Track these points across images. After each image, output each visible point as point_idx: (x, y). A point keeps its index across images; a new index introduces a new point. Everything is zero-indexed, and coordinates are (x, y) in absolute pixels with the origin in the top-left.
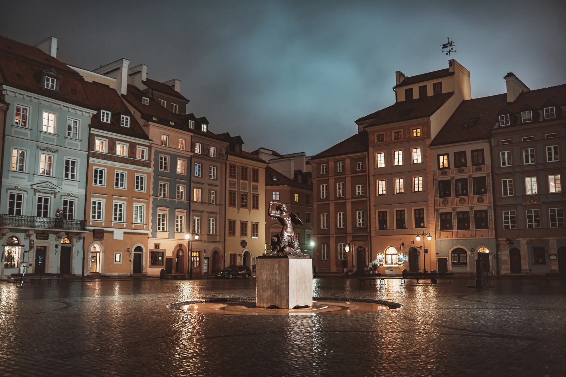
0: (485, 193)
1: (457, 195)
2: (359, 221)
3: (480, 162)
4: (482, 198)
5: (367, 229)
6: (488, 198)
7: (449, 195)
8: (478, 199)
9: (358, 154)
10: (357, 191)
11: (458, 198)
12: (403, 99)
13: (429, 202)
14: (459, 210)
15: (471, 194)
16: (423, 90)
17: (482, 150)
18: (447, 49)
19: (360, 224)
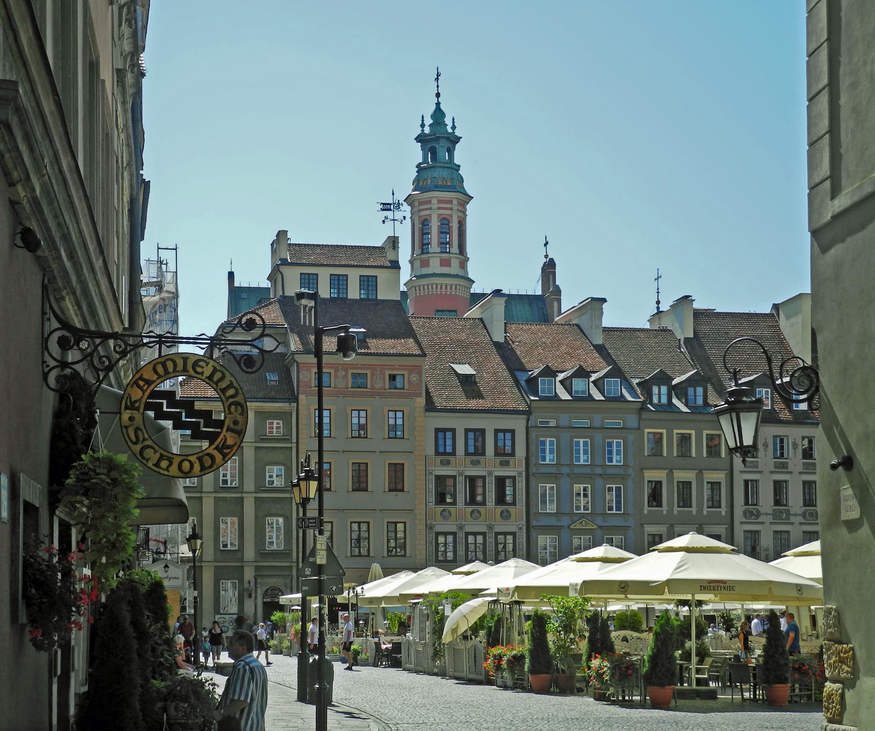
0: (514, 503)
4: (508, 511)
8: (502, 512)
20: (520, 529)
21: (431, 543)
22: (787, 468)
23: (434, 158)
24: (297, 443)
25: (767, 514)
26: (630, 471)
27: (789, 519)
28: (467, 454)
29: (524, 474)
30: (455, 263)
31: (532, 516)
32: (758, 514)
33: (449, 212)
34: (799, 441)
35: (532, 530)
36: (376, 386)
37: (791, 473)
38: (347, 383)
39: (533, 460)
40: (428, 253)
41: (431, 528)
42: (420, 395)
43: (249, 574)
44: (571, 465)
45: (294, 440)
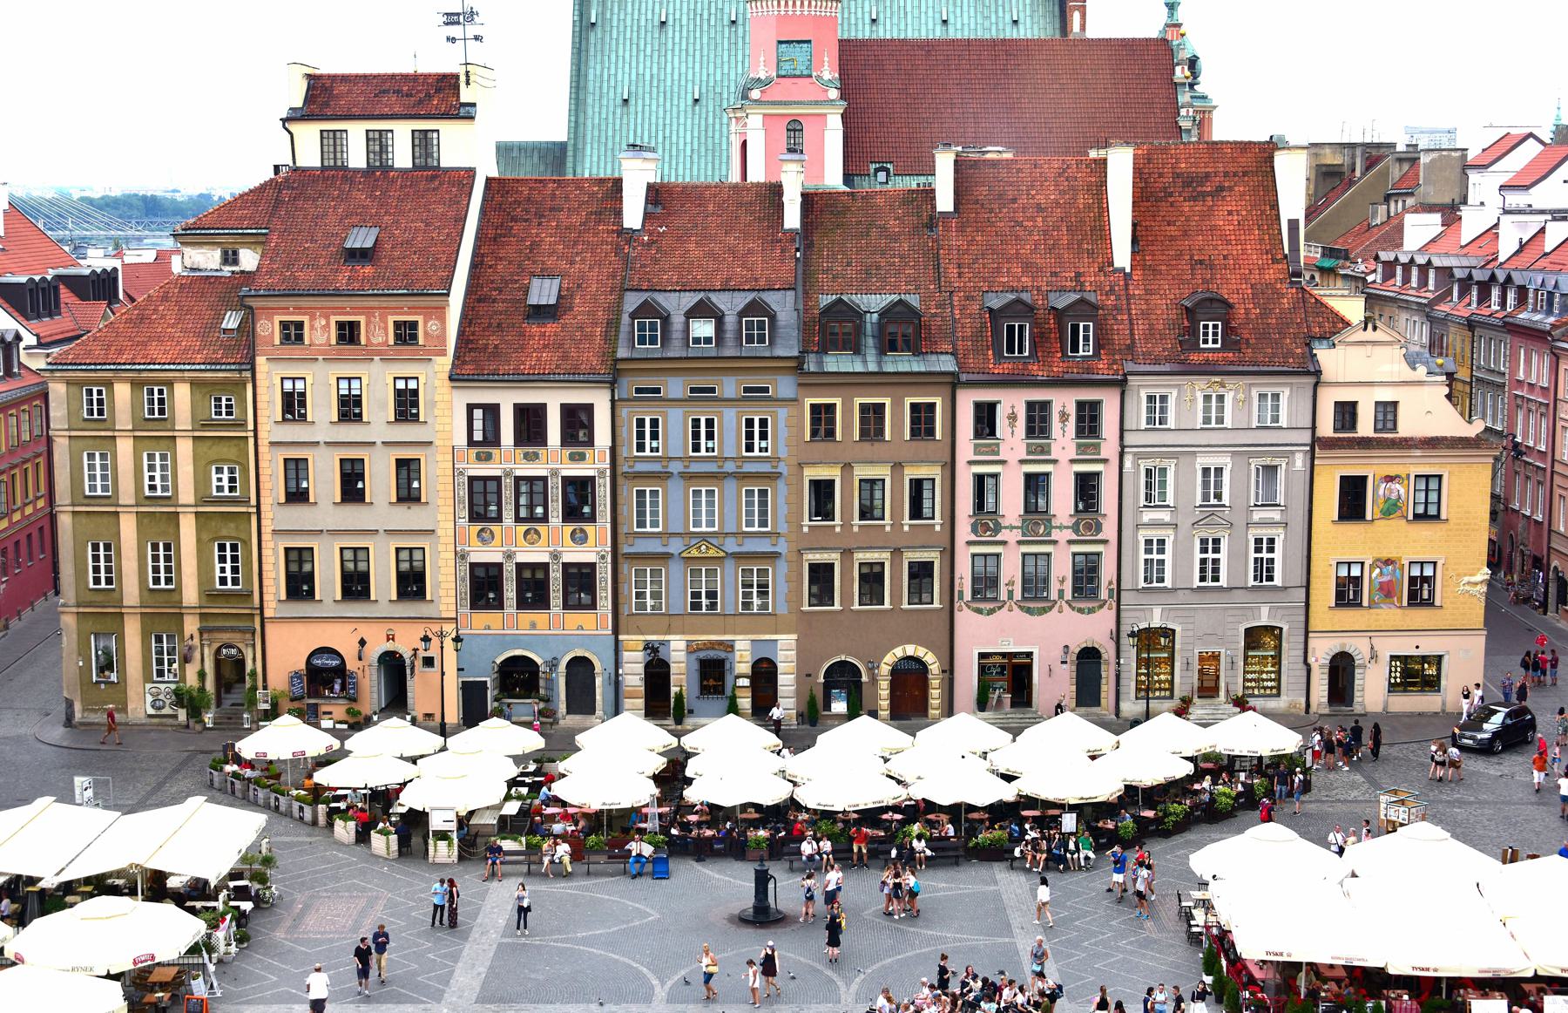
0: (592, 518)
2: (223, 570)
4: (582, 531)
5: (250, 595)
6: (599, 532)
8: (573, 533)
9: (221, 375)
10: (215, 483)
11: (522, 528)
12: (310, 157)
13: (440, 532)
14: (522, 558)
15: (556, 517)
16: (378, 144)
17: (589, 409)
18: (455, 31)
19: (223, 581)
20: (603, 557)
21: (463, 580)
22: (1049, 453)
24: (255, 430)
25: (1012, 528)
26: (782, 468)
27: (1049, 534)
31: (621, 539)
32: (998, 528)
35: (621, 560)
36: (374, 341)
37: (1055, 462)
38: (329, 339)
39: (623, 452)
41: (463, 557)
42: (443, 353)
43: (191, 625)
45: (251, 426)
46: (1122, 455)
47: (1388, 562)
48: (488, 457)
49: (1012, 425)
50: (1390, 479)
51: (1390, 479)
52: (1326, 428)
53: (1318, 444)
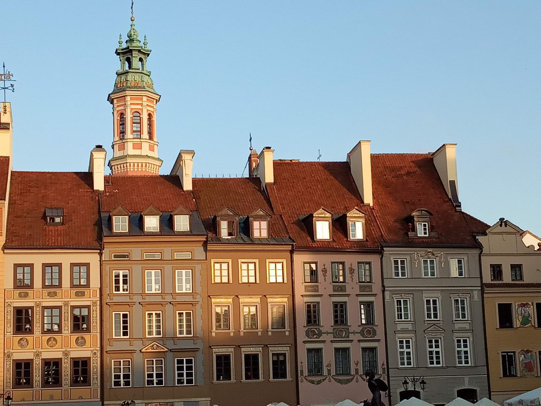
0: (88, 330)
1: (43, 332)
3: (83, 282)
4: (82, 338)
7: (31, 331)
8: (77, 339)
11: (46, 337)
20: (95, 354)
21: (8, 370)
23: (130, 67)
25: (328, 333)
26: (198, 298)
27: (348, 337)
28: (44, 286)
29: (98, 303)
30: (145, 146)
31: (105, 342)
32: (320, 334)
33: (140, 107)
34: (355, 266)
37: (348, 295)
39: (106, 291)
40: (124, 139)
41: (9, 356)
44: (143, 294)
46: (383, 291)
47: (528, 351)
48: (26, 295)
49: (325, 276)
50: (523, 305)
51: (523, 305)
52: (487, 278)
53: (483, 286)
